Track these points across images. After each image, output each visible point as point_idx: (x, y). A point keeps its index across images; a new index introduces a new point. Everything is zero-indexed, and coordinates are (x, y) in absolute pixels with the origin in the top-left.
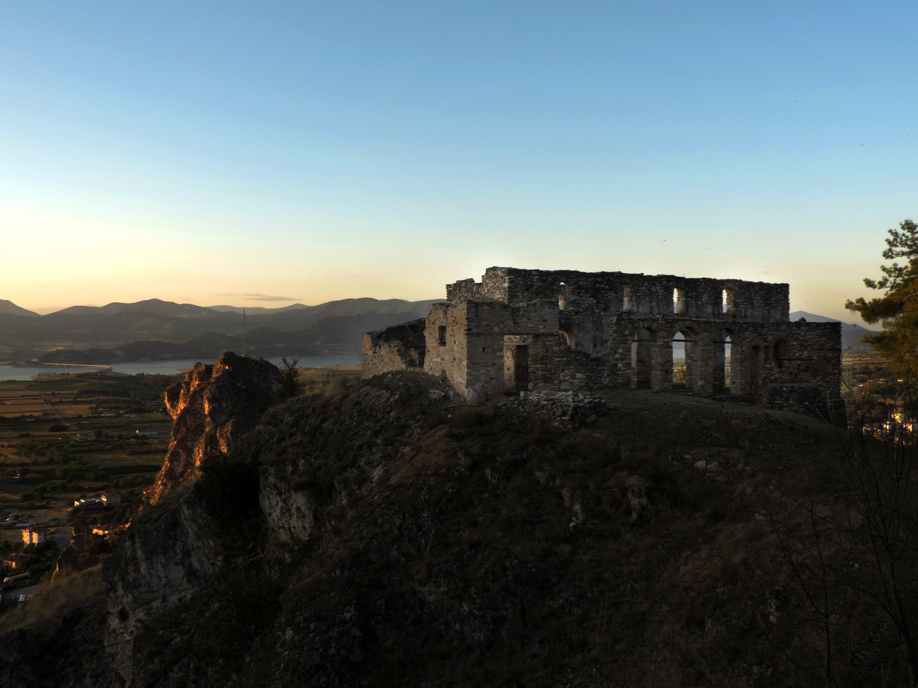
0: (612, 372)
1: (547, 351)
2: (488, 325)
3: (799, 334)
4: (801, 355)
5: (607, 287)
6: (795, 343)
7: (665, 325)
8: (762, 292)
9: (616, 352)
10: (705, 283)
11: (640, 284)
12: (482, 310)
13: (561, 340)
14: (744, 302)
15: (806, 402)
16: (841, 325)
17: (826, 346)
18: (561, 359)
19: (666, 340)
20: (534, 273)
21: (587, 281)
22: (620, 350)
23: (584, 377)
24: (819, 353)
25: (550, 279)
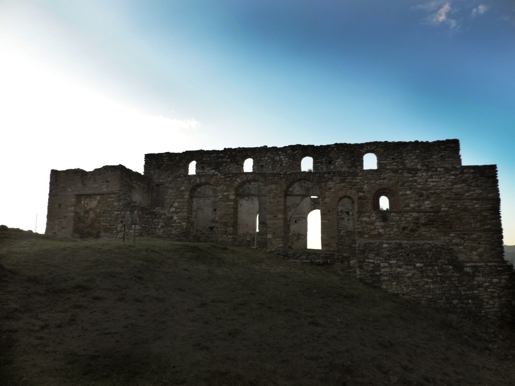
0: (168, 224)
1: (108, 206)
2: (64, 187)
3: (416, 181)
4: (419, 206)
5: (229, 160)
6: (408, 192)
7: (224, 180)
8: (418, 151)
9: (172, 206)
10: (338, 149)
11: (263, 155)
12: (60, 176)
13: (121, 196)
14: (392, 163)
15: (417, 263)
16: (496, 168)
17: (467, 194)
18: (119, 213)
19: (226, 193)
20: (164, 155)
21: (210, 157)
22: (176, 204)
23: (140, 228)
24: (452, 203)
25: (178, 158)
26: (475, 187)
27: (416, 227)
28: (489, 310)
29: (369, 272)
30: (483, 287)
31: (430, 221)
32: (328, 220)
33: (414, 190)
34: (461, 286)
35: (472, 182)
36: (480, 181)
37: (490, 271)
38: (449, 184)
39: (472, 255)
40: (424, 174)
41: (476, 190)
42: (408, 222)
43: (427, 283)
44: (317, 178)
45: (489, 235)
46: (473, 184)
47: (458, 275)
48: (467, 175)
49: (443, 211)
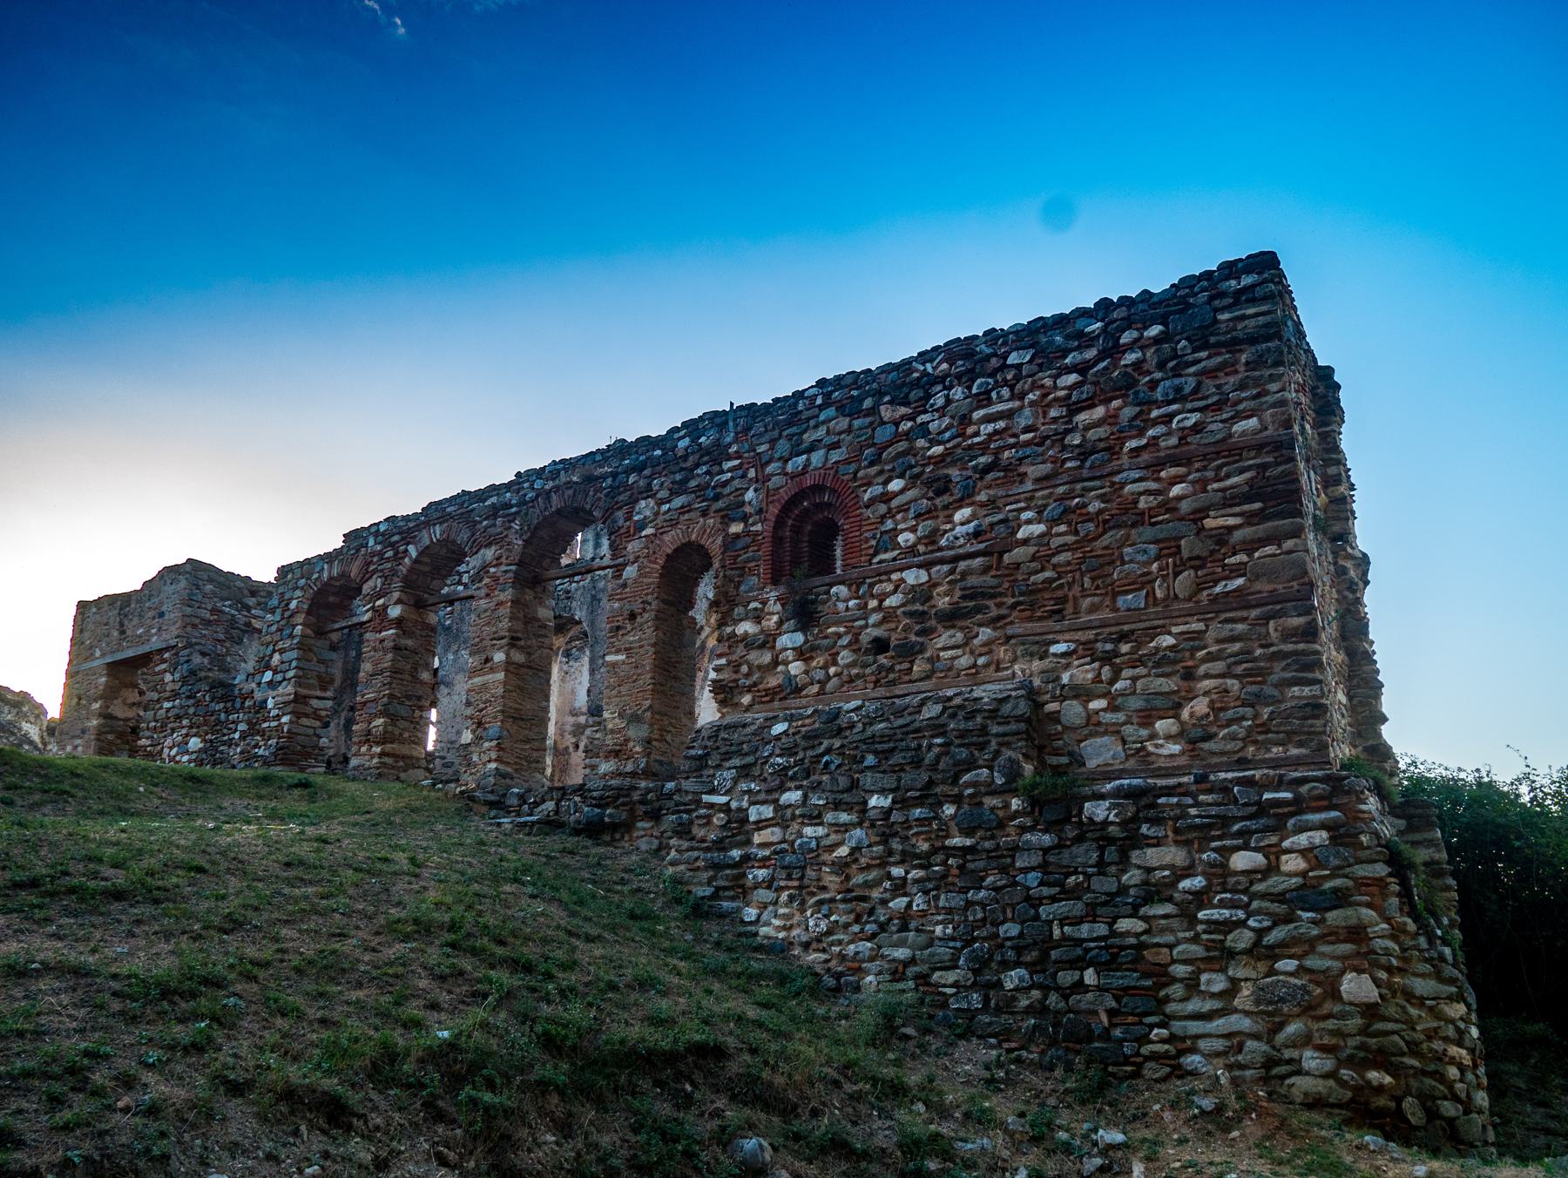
3: (923, 430)
26: (1169, 403)
27: (917, 634)
28: (1195, 1027)
29: (708, 849)
30: (1170, 900)
31: (971, 597)
32: (626, 649)
33: (916, 470)
34: (1054, 899)
35: (1153, 385)
36: (1192, 370)
37: (1214, 811)
38: (1053, 413)
39: (1153, 736)
40: (958, 393)
41: (1171, 416)
42: (889, 616)
43: (900, 887)
44: (606, 496)
45: (1240, 627)
46: (1159, 394)
47: (1047, 839)
48: (1130, 358)
49: (1025, 542)
